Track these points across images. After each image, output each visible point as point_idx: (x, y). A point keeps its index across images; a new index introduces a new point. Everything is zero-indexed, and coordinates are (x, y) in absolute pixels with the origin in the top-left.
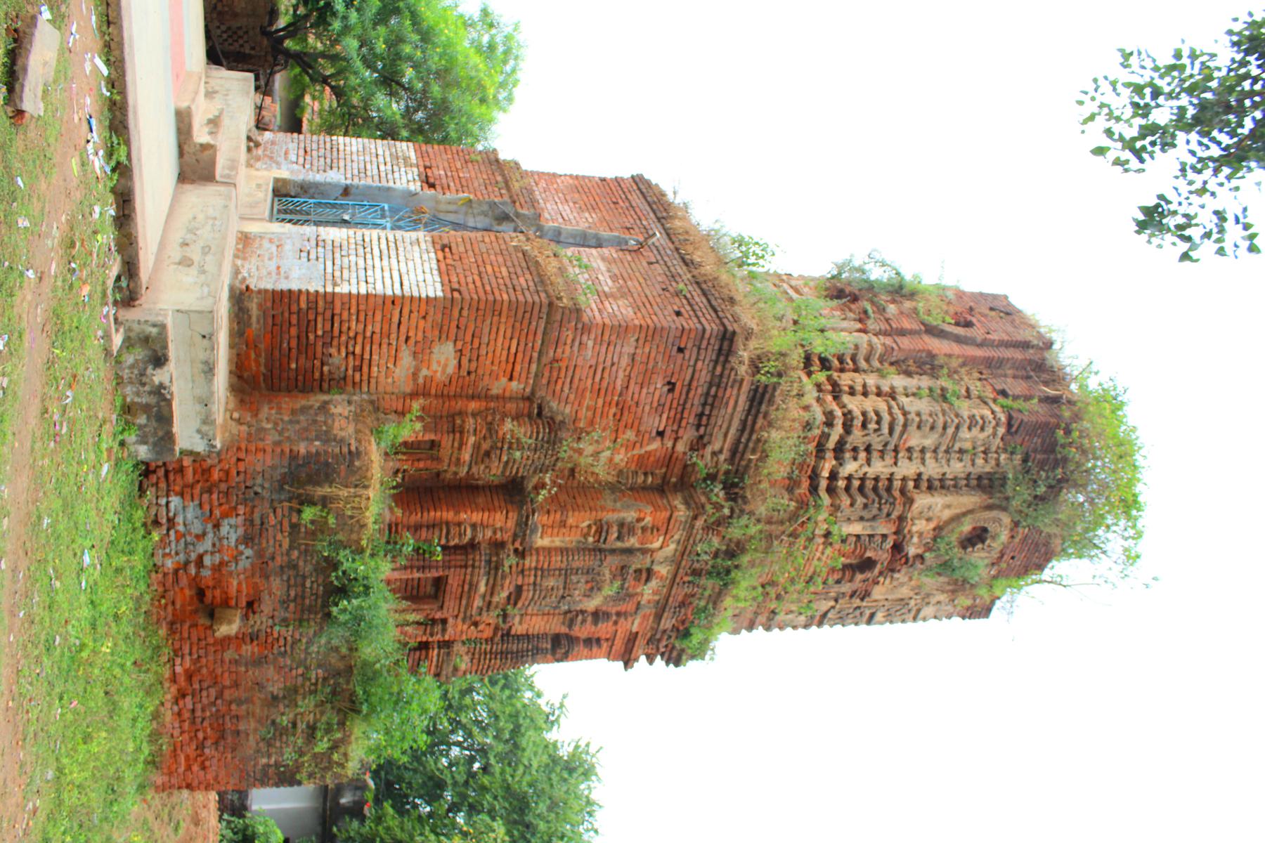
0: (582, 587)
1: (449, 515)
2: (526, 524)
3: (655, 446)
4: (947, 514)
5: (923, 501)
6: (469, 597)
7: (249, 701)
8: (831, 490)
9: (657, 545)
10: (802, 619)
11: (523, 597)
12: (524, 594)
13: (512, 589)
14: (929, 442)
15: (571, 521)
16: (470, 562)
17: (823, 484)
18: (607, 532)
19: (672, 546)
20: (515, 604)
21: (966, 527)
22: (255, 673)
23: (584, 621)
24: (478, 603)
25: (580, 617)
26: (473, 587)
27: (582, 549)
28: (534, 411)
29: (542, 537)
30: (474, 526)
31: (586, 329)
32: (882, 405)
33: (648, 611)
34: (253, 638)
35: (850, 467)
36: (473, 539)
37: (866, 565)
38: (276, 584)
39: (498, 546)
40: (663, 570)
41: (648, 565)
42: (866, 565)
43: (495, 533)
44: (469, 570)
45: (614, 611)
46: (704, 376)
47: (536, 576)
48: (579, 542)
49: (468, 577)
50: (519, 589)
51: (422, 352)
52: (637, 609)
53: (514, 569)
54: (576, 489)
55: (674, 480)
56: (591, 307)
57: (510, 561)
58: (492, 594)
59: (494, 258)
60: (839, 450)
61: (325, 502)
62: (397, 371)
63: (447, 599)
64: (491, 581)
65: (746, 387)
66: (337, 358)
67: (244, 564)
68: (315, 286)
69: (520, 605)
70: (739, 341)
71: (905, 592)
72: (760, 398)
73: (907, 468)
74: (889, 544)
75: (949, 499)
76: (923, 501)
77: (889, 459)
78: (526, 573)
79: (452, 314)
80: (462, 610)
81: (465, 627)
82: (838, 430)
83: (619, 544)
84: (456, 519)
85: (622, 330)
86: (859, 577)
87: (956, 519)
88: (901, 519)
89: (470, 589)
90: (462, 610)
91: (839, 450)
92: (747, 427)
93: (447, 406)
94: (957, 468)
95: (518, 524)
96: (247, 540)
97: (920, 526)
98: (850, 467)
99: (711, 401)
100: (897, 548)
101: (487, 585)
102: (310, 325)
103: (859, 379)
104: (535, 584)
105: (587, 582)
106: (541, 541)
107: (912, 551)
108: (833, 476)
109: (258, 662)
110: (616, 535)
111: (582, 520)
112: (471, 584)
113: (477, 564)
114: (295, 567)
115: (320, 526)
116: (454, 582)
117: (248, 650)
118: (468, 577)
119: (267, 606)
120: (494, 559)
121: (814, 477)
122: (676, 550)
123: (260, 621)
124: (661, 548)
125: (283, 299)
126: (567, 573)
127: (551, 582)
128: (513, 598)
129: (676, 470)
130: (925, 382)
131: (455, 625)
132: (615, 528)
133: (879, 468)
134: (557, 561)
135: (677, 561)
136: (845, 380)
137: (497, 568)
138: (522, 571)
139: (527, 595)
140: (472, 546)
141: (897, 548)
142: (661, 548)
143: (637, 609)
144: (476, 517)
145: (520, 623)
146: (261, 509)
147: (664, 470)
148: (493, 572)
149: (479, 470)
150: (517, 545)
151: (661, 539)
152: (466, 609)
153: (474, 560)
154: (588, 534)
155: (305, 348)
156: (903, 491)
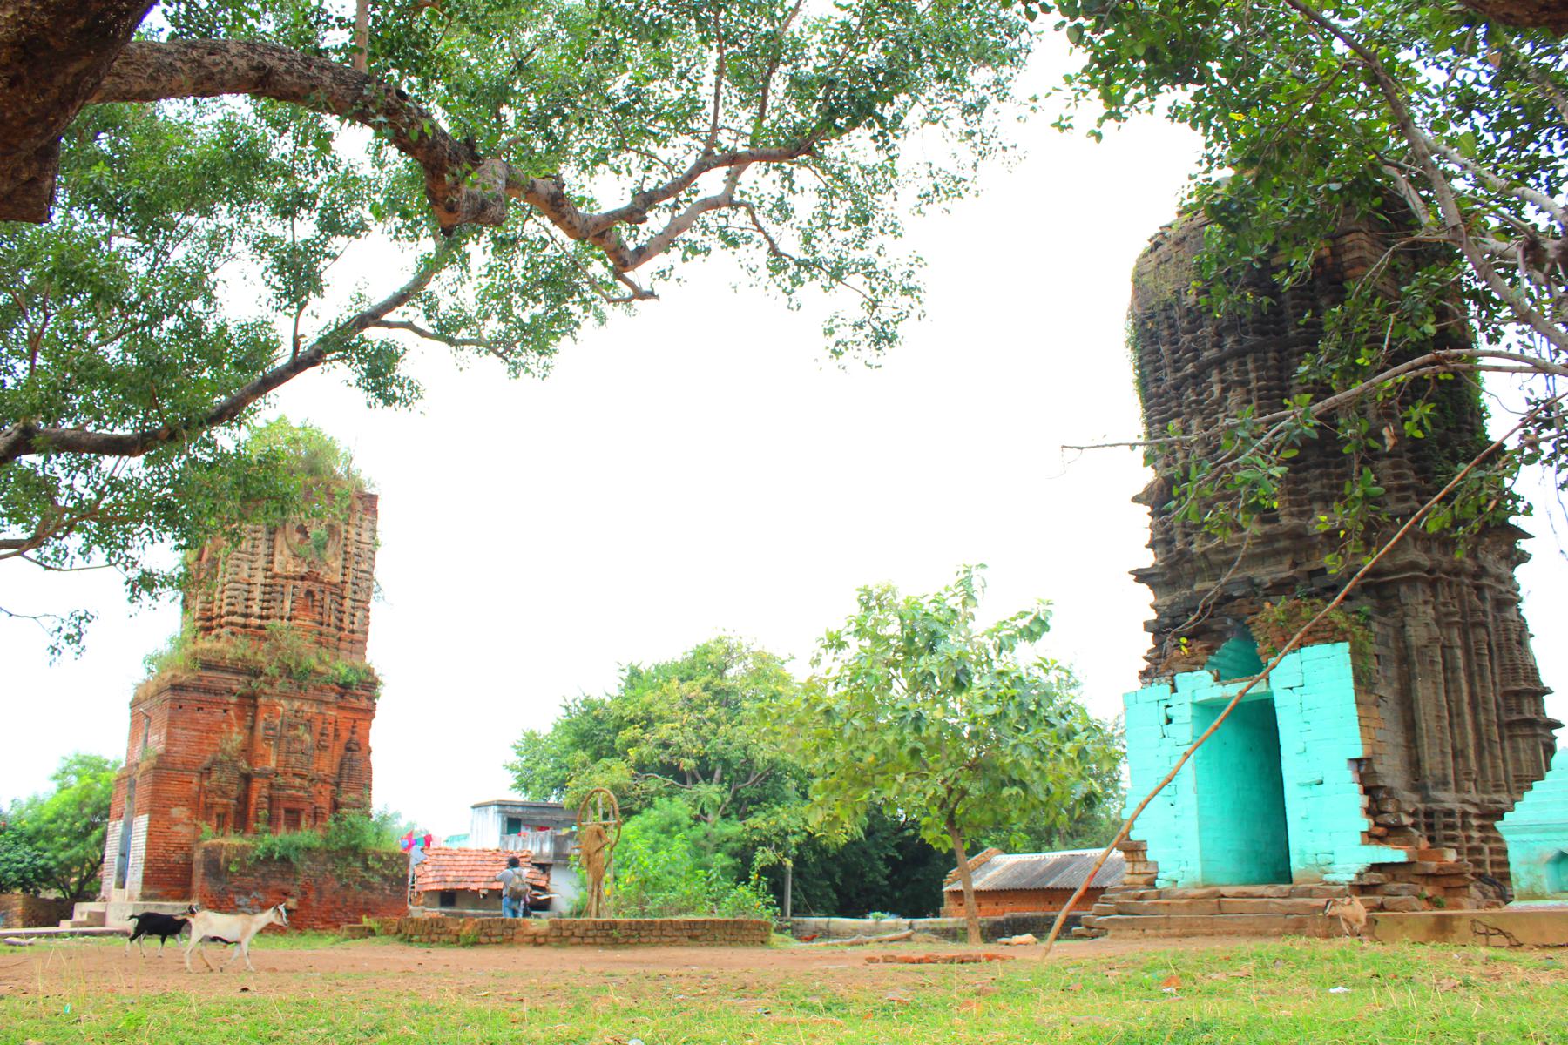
0: (297, 746)
1: (252, 809)
3: (232, 713)
4: (287, 552)
5: (277, 569)
7: (345, 897)
8: (268, 618)
10: (359, 614)
14: (245, 566)
17: (264, 622)
21: (298, 537)
22: (327, 895)
24: (301, 793)
27: (278, 746)
28: (207, 772)
31: (167, 751)
32: (227, 593)
33: (323, 709)
34: (304, 893)
35: (256, 609)
37: (310, 593)
38: (272, 883)
39: (272, 786)
40: (297, 704)
42: (310, 593)
46: (195, 695)
51: (175, 822)
54: (248, 751)
56: (160, 748)
57: (280, 780)
59: (143, 790)
60: (247, 616)
61: (228, 862)
62: (183, 832)
65: (203, 673)
66: (176, 857)
67: (260, 896)
68: (141, 868)
70: (178, 681)
71: (337, 564)
72: (207, 666)
73: (260, 578)
74: (299, 583)
75: (277, 553)
76: (277, 569)
77: (252, 588)
79: (158, 809)
82: (235, 619)
85: (169, 735)
86: (318, 597)
87: (289, 546)
88: (287, 578)
91: (247, 616)
92: (225, 669)
93: (202, 808)
94: (262, 548)
96: (248, 894)
97: (291, 568)
98: (256, 609)
99: (207, 690)
100: (303, 578)
102: (160, 870)
103: (217, 603)
106: (273, 764)
107: (305, 569)
108: (261, 617)
109: (320, 892)
111: (262, 747)
114: (263, 876)
115: (242, 864)
116: (288, 805)
117: (312, 896)
119: (286, 887)
121: (261, 627)
123: (295, 890)
125: (147, 880)
126: (288, 752)
130: (221, 566)
133: (257, 594)
134: (282, 758)
135: (291, 698)
136: (216, 611)
139: (297, 770)
140: (270, 798)
141: (303, 578)
146: (230, 887)
149: (234, 795)
155: (170, 871)
156: (273, 577)
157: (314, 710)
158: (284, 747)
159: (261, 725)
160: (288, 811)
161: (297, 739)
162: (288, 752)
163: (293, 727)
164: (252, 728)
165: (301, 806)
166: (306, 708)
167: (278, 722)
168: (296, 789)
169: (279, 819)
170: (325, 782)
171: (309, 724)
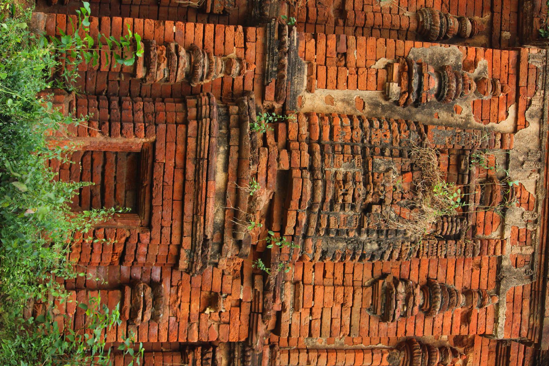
2: (281, 44)
6: (198, 191)
9: (507, 125)
11: (296, 195)
12: (297, 184)
13: (273, 180)
15: (354, 55)
16: (193, 112)
18: (421, 74)
19: (534, 127)
20: (282, 232)
23: (409, 294)
24: (214, 212)
25: (401, 288)
26: (203, 163)
29: (310, 90)
30: (191, 50)
33: (517, 284)
36: (191, 75)
39: (233, 96)
41: (500, 169)
43: (228, 64)
44: (193, 124)
45: (458, 288)
47: (311, 153)
48: (376, 105)
49: (192, 143)
50: (285, 179)
52: (498, 282)
53: (270, 140)
55: (506, 34)
57: (260, 124)
58: (239, 180)
63: (157, 202)
64: (234, 156)
69: (289, 231)
78: (294, 145)
80: (187, 228)
81: (196, 307)
83: (444, 115)
84: (159, 32)
89: (197, 172)
90: (187, 228)
95: (266, 50)
101: (226, 168)
104: (312, 169)
105: (403, 173)
106: (315, 100)
110: (434, 84)
111: (373, 55)
112: (198, 160)
113: (205, 110)
116: (166, 159)
118: (192, 143)
120: (234, 109)
122: (541, 134)
124: (515, 131)
127: (342, 168)
128: (276, 213)
129: (506, 16)
131: (177, 302)
132: (432, 70)
137: (240, 124)
138: (287, 146)
139: (302, 186)
142: (515, 131)
143: (498, 282)
144: (193, 32)
145: (296, 308)
147: (487, 17)
148: (234, 132)
150: (270, 94)
151: (512, 110)
152: (194, 224)
153: (198, 107)
154: (389, 80)
157: (511, 250)
158: (379, 136)
159: (454, 53)
160: (140, 163)
161: (420, 186)
162: (366, 153)
163: (459, 164)
164: (423, 34)
165: (164, 214)
166: (516, 216)
167: (465, 109)
168: (228, 185)
169: (107, 125)
170: (256, 314)
171: (456, 231)
